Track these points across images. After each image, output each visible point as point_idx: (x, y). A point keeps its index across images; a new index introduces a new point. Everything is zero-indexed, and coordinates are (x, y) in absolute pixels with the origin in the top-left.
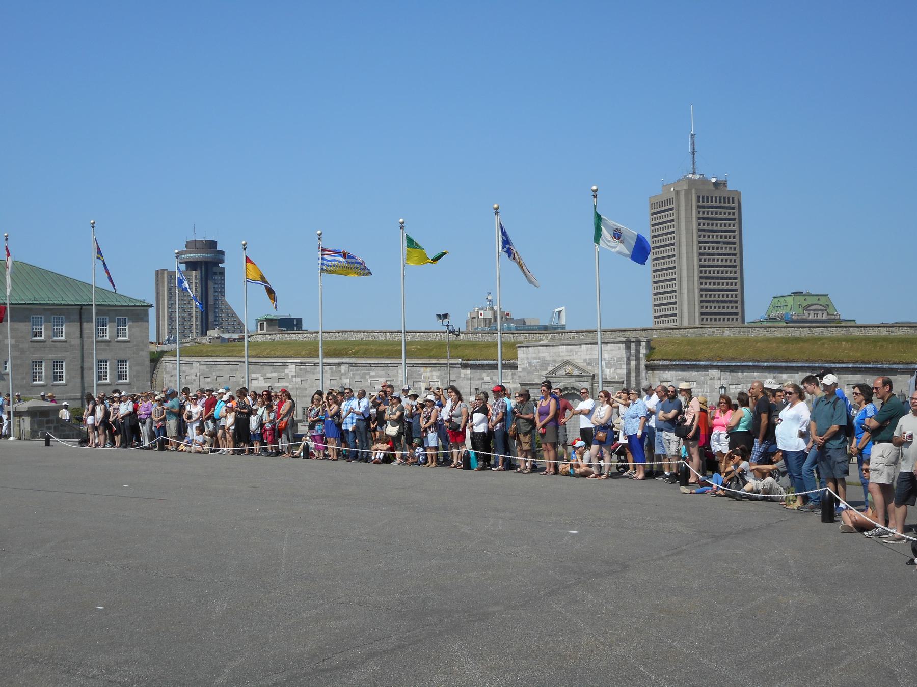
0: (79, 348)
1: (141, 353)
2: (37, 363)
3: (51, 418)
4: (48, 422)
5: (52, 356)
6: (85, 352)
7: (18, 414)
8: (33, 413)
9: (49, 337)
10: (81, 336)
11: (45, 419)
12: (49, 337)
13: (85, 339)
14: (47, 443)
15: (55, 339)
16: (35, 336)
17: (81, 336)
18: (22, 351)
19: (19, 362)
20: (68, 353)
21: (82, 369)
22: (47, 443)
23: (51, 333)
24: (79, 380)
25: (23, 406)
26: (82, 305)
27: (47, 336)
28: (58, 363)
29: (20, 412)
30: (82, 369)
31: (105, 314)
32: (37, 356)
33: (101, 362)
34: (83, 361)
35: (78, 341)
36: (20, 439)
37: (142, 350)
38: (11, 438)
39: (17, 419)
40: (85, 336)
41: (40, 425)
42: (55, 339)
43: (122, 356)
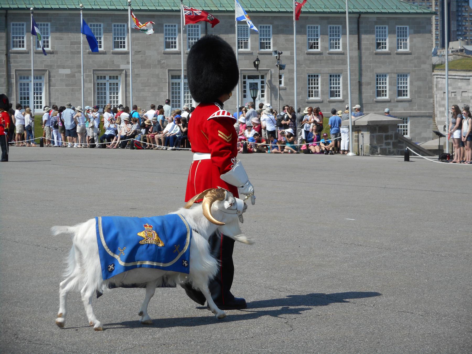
1: (423, 66)
2: (313, 77)
3: (390, 133)
4: (387, 138)
5: (327, 69)
6: (363, 65)
7: (356, 129)
8: (372, 128)
9: (326, 49)
10: (359, 48)
11: (384, 134)
12: (326, 49)
13: (363, 51)
14: (407, 159)
15: (332, 50)
16: (311, 48)
17: (359, 48)
21: (360, 84)
22: (407, 159)
23: (327, 45)
25: (364, 120)
26: (360, 13)
27: (324, 48)
28: (334, 77)
29: (358, 127)
30: (360, 84)
31: (384, 23)
32: (313, 70)
33: (380, 77)
34: (361, 75)
36: (358, 155)
37: (424, 63)
38: (350, 154)
39: (355, 134)
40: (363, 47)
41: (379, 140)
42: (332, 50)
43: (402, 69)
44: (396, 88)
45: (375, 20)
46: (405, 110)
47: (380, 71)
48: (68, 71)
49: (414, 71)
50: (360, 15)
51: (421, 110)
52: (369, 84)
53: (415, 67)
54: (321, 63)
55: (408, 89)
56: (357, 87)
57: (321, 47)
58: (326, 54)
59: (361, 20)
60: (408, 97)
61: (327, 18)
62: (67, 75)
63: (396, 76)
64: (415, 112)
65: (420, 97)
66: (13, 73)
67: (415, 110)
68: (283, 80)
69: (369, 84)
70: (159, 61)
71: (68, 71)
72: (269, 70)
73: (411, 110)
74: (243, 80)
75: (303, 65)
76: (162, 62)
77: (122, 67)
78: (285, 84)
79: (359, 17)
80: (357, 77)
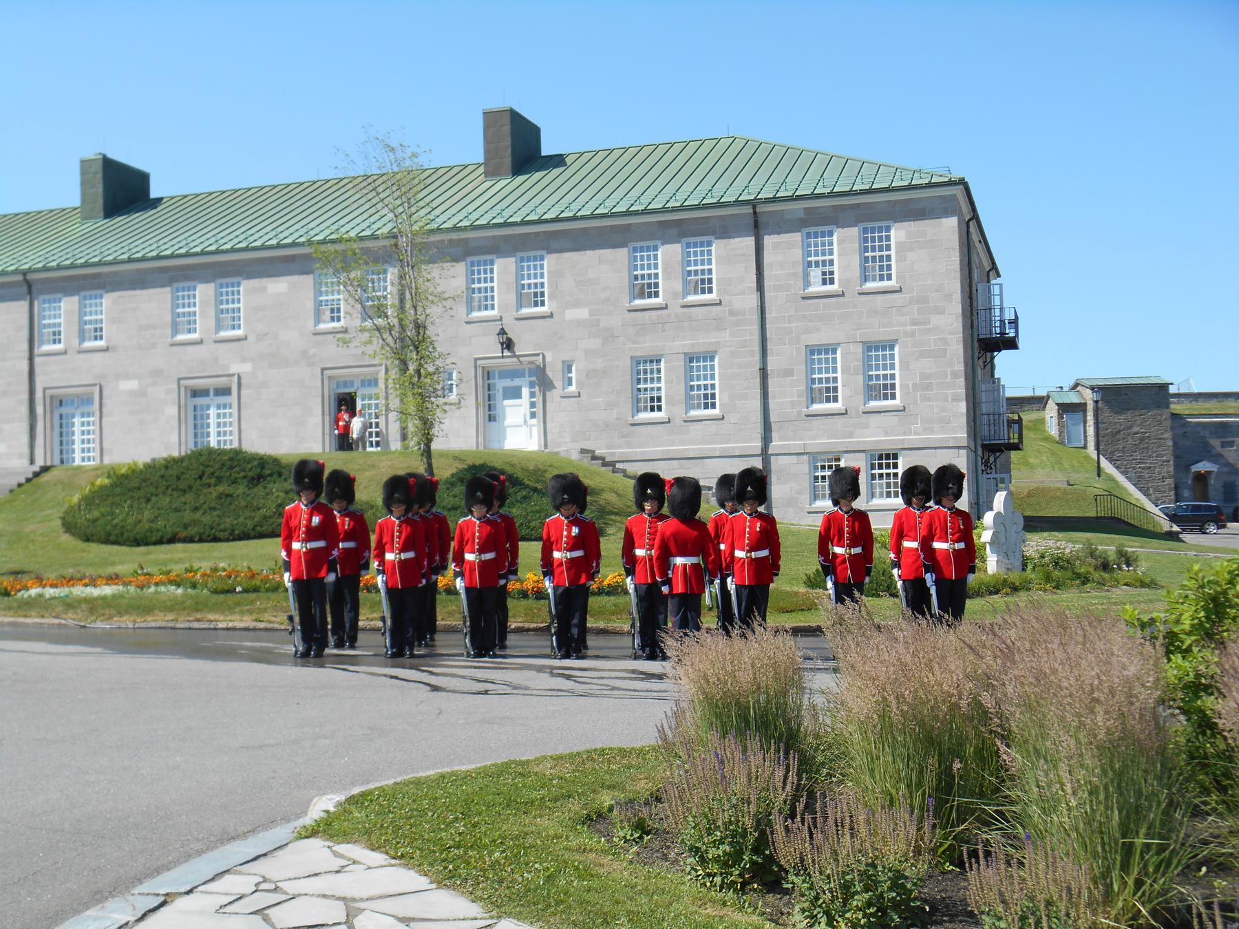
0: (756, 317)
1: (935, 320)
2: (644, 366)
10: (760, 287)
16: (641, 295)
17: (760, 287)
18: (609, 336)
19: (599, 364)
20: (725, 336)
21: (764, 372)
24: (756, 403)
30: (764, 372)
32: (646, 347)
35: (754, 299)
40: (767, 283)
43: (878, 332)
44: (860, 379)
45: (801, 215)
46: (887, 434)
47: (815, 339)
48: (132, 385)
49: (913, 334)
50: (754, 207)
51: (932, 431)
52: (788, 373)
53: (914, 323)
54: (664, 331)
55: (897, 381)
56: (757, 381)
57: (664, 291)
58: (675, 309)
59: (761, 220)
60: (897, 402)
61: (679, 222)
62: (131, 393)
63: (860, 349)
64: (913, 438)
65: (929, 400)
66: (39, 395)
67: (916, 434)
68: (573, 375)
69: (788, 373)
70: (304, 353)
71: (132, 385)
72: (538, 355)
73: (905, 433)
74: (487, 382)
75: (622, 339)
76: (312, 352)
77: (234, 369)
78: (579, 383)
79: (755, 213)
80: (757, 357)
